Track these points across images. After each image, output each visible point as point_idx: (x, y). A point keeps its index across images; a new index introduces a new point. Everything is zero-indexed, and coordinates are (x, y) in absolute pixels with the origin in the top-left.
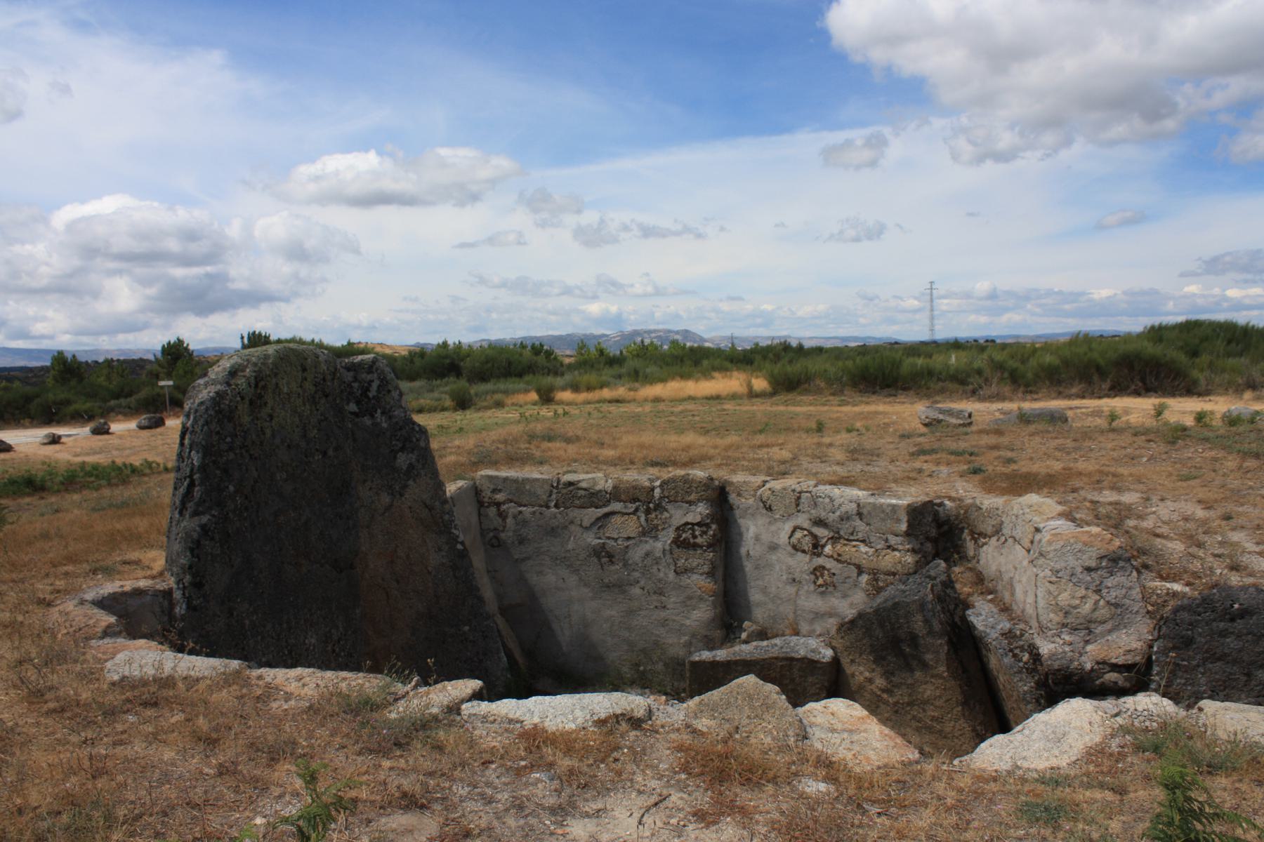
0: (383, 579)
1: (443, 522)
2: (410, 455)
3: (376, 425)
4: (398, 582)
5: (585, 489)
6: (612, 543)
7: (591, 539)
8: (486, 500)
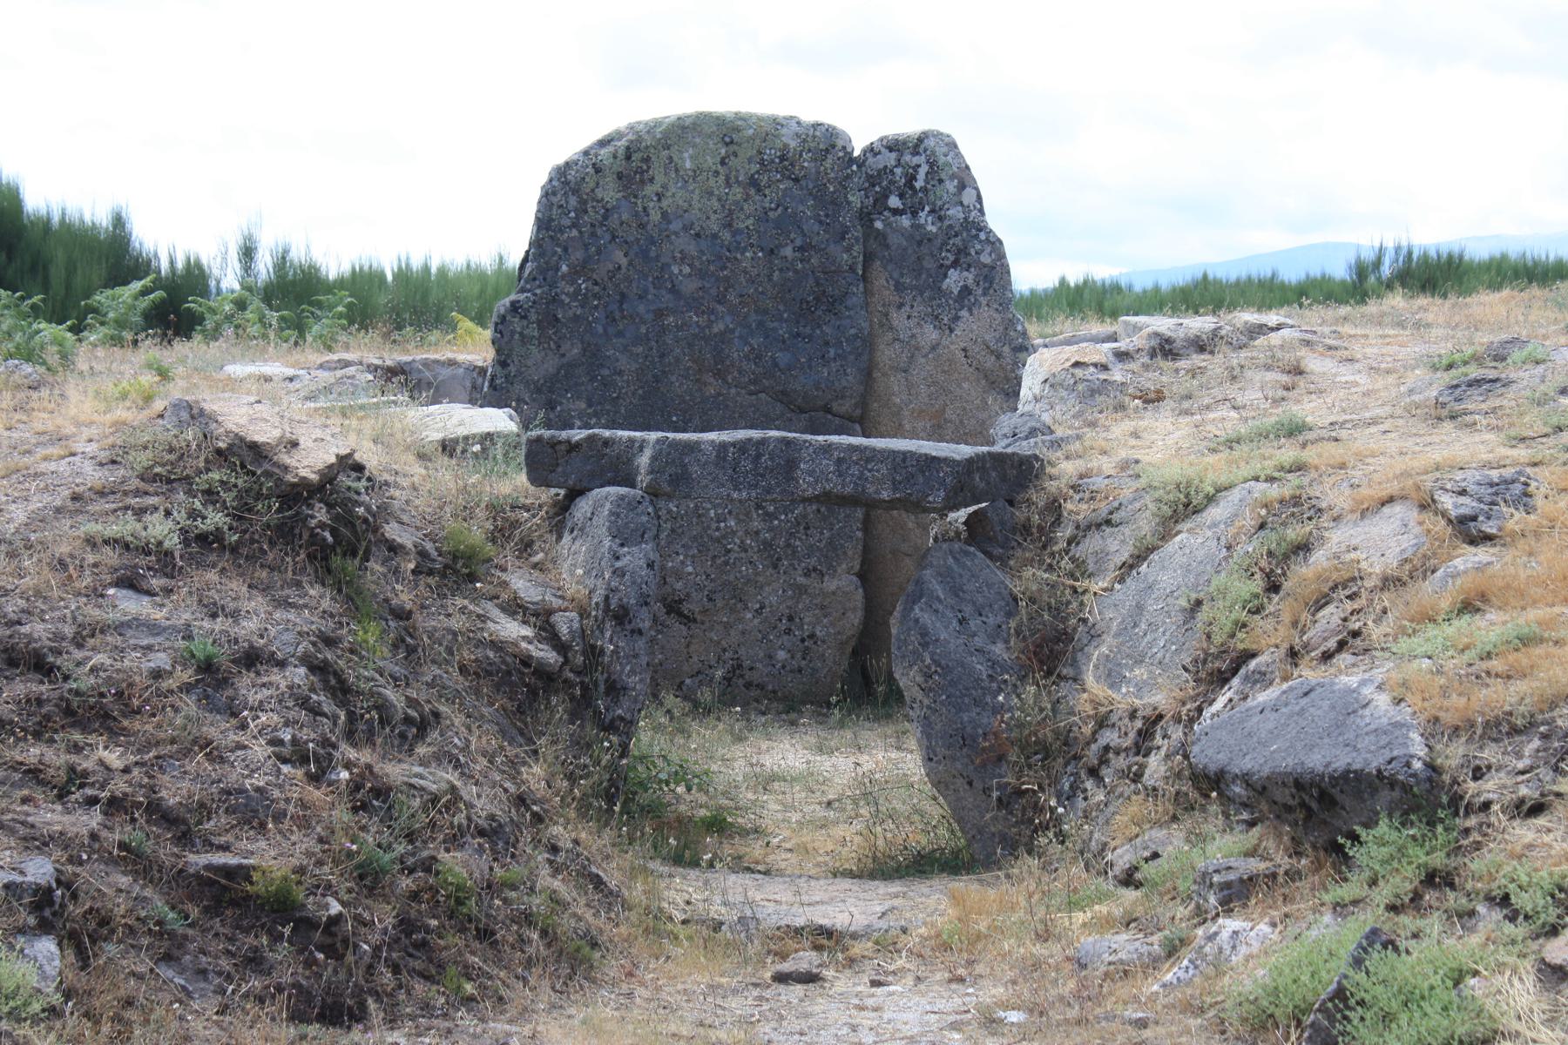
2: (965, 274)
3: (917, 227)
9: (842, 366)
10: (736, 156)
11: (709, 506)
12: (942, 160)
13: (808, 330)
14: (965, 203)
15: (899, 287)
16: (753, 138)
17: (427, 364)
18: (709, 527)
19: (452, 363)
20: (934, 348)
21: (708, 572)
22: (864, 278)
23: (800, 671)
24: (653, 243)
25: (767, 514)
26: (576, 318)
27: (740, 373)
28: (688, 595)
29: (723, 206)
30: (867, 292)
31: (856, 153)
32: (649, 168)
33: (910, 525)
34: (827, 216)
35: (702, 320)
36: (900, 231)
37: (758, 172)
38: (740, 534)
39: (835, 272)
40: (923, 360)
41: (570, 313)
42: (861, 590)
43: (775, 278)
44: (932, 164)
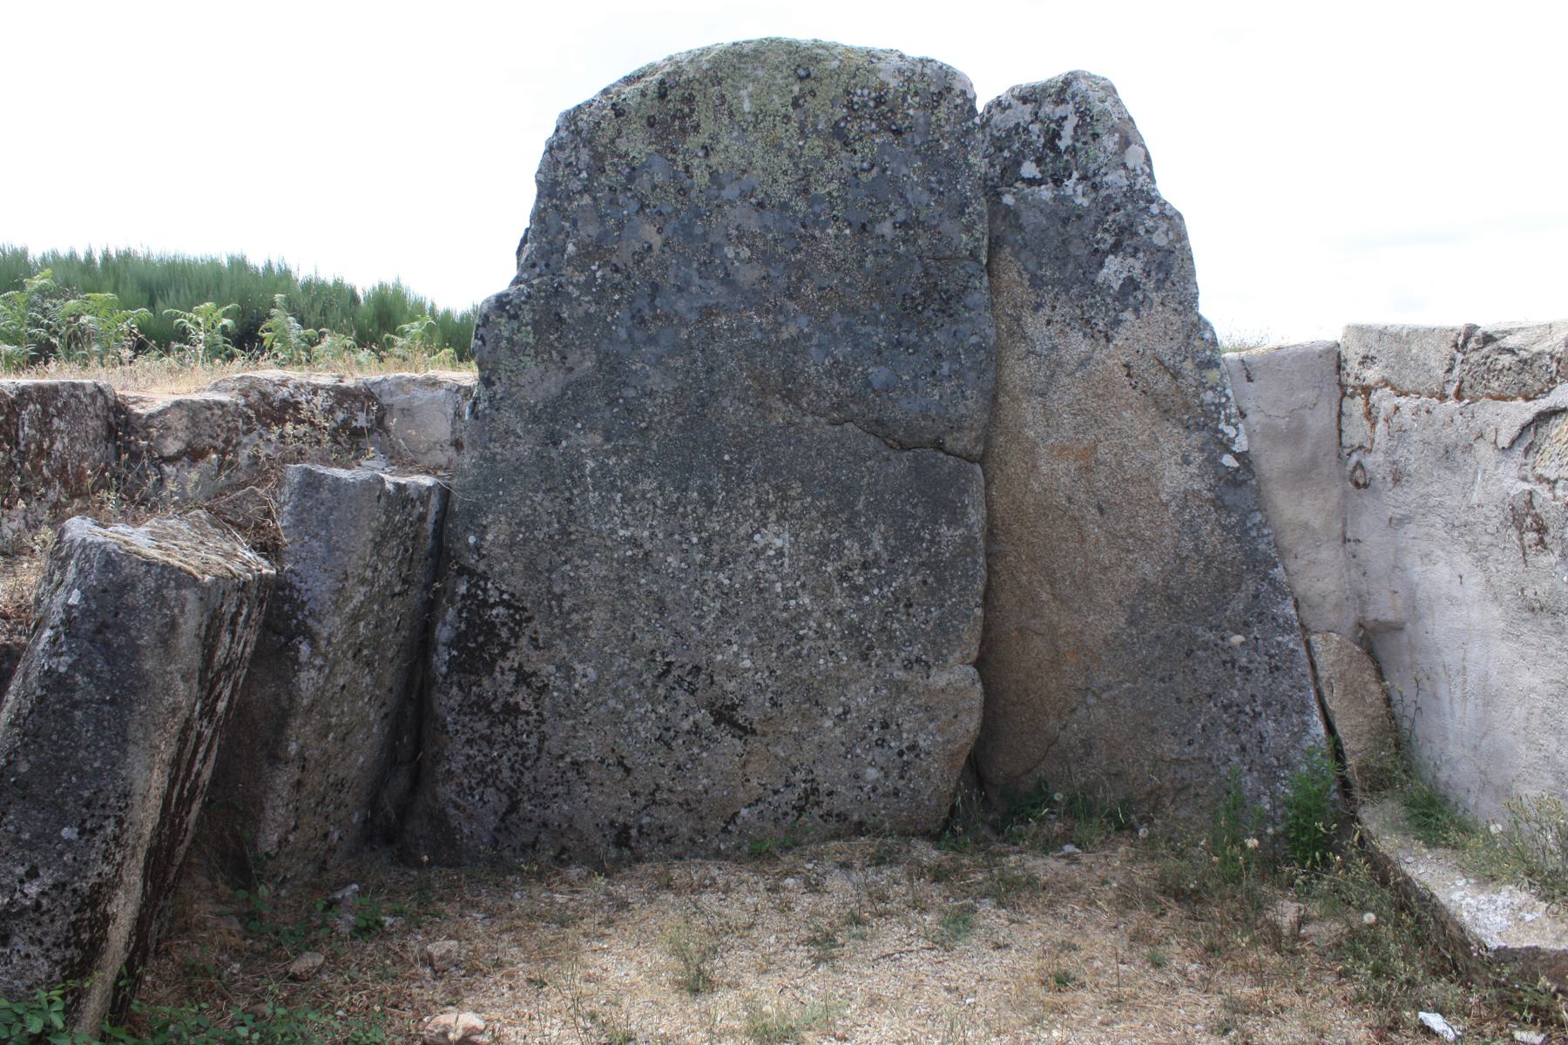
0: (1069, 500)
1: (1201, 405)
2: (1130, 261)
3: (1061, 200)
4: (1101, 511)
5: (1511, 351)
6: (1543, 491)
7: (1509, 481)
8: (1351, 380)
9: (959, 386)
10: (813, 93)
11: (774, 577)
12: (1097, 107)
13: (913, 337)
14: (1130, 165)
15: (1036, 282)
16: (837, 72)
17: (400, 384)
18: (774, 607)
19: (434, 383)
20: (1082, 364)
21: (773, 666)
22: (989, 269)
23: (896, 794)
24: (699, 216)
25: (854, 587)
26: (588, 318)
27: (818, 394)
28: (744, 699)
29: (796, 164)
30: (994, 290)
32: (692, 111)
33: (1044, 596)
34: (940, 182)
35: (766, 321)
36: (1039, 206)
37: (844, 118)
38: (817, 614)
39: (950, 258)
40: (1067, 380)
41: (581, 311)
42: (979, 686)
43: (868, 265)
44: (1084, 114)
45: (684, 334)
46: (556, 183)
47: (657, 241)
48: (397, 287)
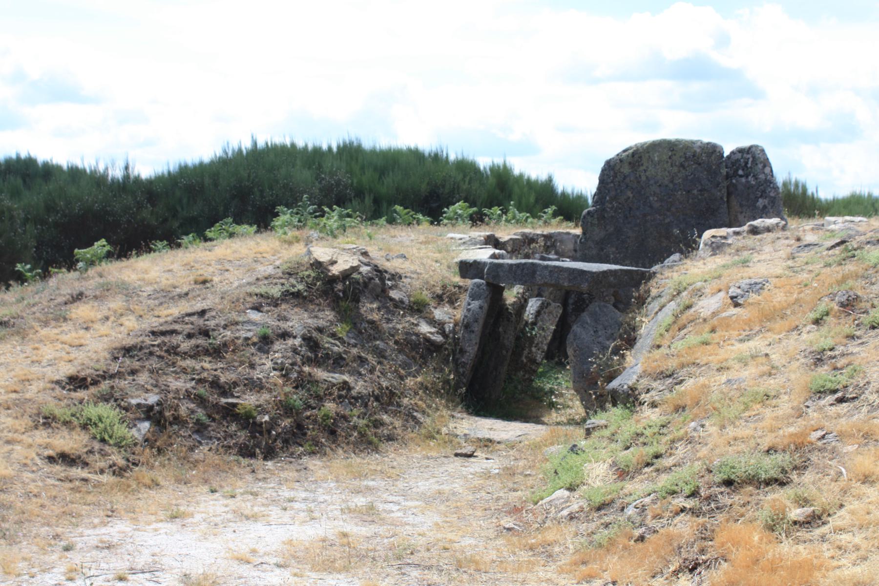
3: (748, 182)
10: (675, 155)
12: (757, 156)
15: (741, 206)
16: (682, 149)
17: (559, 233)
19: (568, 234)
22: (728, 201)
26: (612, 217)
30: (729, 207)
31: (725, 155)
35: (661, 218)
41: (610, 215)
44: (754, 157)
45: (638, 221)
46: (604, 180)
47: (631, 196)
48: (505, 166)
